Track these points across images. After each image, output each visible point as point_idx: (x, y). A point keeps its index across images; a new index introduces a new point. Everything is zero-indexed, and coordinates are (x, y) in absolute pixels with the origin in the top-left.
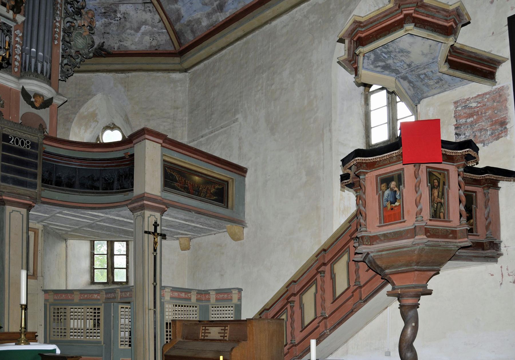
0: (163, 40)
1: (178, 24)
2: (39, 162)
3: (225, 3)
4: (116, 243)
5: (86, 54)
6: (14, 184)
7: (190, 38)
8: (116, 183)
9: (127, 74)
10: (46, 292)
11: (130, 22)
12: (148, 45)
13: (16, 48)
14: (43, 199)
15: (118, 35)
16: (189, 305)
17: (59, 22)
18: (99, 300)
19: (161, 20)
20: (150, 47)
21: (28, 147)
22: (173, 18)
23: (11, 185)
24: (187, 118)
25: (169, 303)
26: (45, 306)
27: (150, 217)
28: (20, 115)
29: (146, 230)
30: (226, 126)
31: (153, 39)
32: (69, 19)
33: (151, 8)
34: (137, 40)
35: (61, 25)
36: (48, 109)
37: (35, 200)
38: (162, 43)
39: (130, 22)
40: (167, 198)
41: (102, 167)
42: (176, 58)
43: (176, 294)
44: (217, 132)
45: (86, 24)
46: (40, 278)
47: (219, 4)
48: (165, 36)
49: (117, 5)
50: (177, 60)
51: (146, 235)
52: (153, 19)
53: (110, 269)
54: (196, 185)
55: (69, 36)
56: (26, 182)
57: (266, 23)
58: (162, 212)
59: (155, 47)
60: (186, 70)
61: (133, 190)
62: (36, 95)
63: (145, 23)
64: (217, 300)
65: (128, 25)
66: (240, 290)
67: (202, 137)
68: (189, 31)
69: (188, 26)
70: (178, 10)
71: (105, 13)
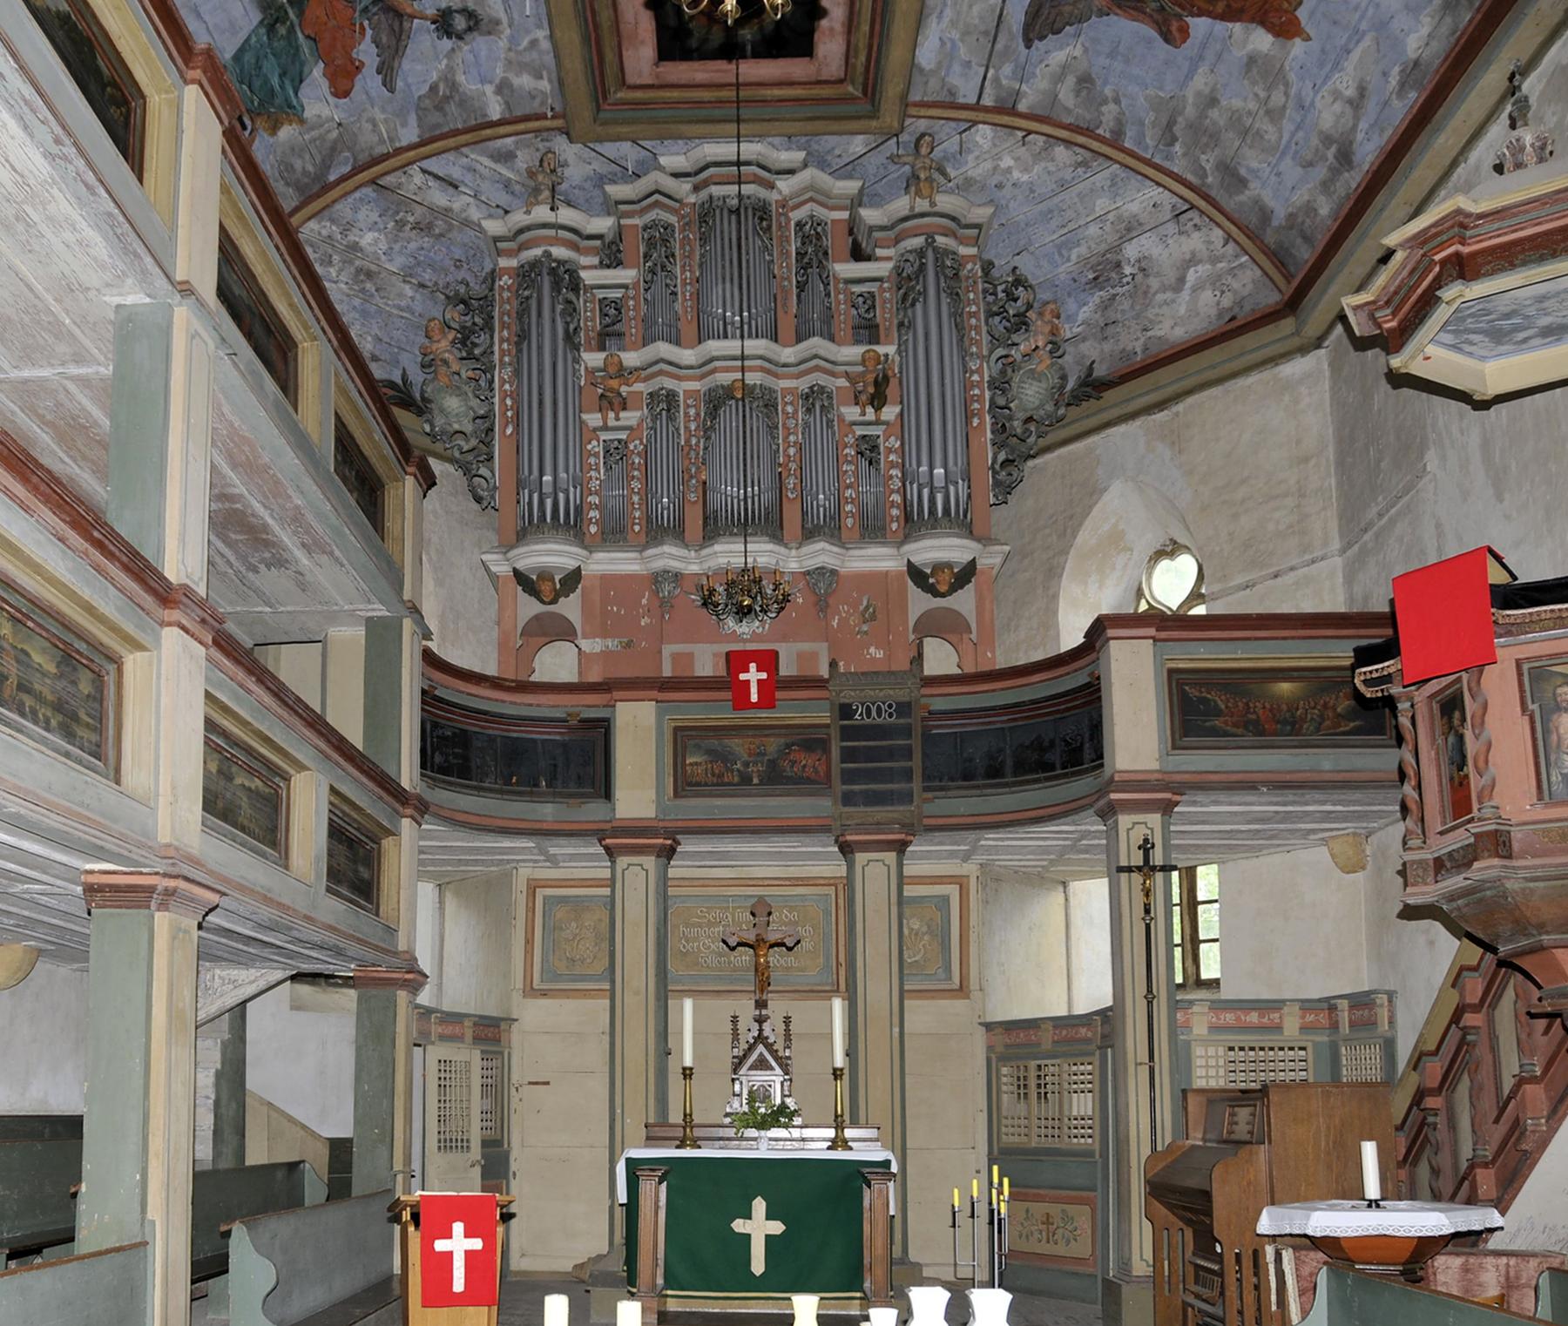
0: (1248, 283)
1: (1269, 231)
2: (916, 743)
3: (1351, 143)
4: (1199, 869)
5: (1049, 416)
6: (866, 805)
7: (1305, 255)
8: (1087, 745)
9: (1175, 409)
10: (989, 1027)
11: (1158, 274)
12: (1213, 312)
13: (891, 477)
14: (926, 821)
15: (1137, 316)
16: (1276, 1045)
17: (977, 371)
18: (1087, 1041)
19: (1229, 237)
20: (1220, 315)
21: (891, 715)
22: (1253, 220)
23: (862, 809)
24: (1333, 481)
25: (1205, 1042)
26: (989, 1060)
27: (1134, 827)
28: (911, 624)
29: (1124, 863)
30: (1407, 491)
31: (1223, 292)
32: (1000, 352)
33: (1197, 220)
34: (1182, 310)
35: (982, 377)
36: (970, 587)
37: (914, 828)
38: (1246, 292)
39: (1158, 274)
40: (1184, 768)
41: (1058, 712)
42: (1283, 322)
43: (1229, 1018)
44: (1393, 511)
45: (1040, 344)
46: (975, 995)
47: (1339, 150)
48: (1249, 273)
49: (1117, 248)
50: (1287, 325)
51: (1124, 876)
52: (1210, 242)
53: (1188, 946)
54: (1284, 707)
55: (1004, 391)
56: (892, 792)
57: (1454, 164)
58: (1167, 808)
59: (1231, 309)
60: (1318, 343)
61: (1102, 765)
62: (938, 567)
63: (1193, 261)
64: (1352, 1024)
65: (1154, 283)
66: (1391, 995)
67: (1366, 530)
68: (1299, 241)
69: (1291, 228)
70: (1257, 201)
71: (1095, 279)
